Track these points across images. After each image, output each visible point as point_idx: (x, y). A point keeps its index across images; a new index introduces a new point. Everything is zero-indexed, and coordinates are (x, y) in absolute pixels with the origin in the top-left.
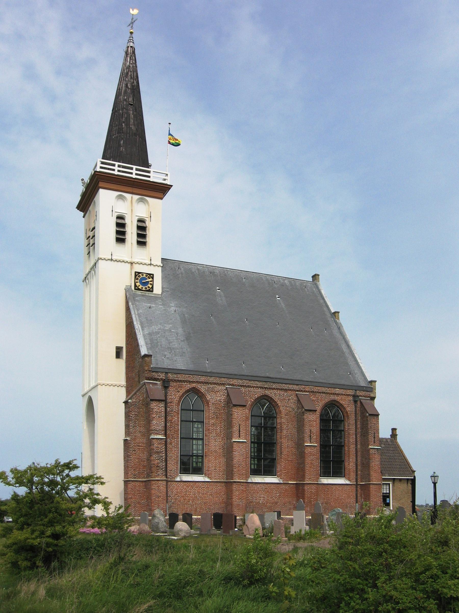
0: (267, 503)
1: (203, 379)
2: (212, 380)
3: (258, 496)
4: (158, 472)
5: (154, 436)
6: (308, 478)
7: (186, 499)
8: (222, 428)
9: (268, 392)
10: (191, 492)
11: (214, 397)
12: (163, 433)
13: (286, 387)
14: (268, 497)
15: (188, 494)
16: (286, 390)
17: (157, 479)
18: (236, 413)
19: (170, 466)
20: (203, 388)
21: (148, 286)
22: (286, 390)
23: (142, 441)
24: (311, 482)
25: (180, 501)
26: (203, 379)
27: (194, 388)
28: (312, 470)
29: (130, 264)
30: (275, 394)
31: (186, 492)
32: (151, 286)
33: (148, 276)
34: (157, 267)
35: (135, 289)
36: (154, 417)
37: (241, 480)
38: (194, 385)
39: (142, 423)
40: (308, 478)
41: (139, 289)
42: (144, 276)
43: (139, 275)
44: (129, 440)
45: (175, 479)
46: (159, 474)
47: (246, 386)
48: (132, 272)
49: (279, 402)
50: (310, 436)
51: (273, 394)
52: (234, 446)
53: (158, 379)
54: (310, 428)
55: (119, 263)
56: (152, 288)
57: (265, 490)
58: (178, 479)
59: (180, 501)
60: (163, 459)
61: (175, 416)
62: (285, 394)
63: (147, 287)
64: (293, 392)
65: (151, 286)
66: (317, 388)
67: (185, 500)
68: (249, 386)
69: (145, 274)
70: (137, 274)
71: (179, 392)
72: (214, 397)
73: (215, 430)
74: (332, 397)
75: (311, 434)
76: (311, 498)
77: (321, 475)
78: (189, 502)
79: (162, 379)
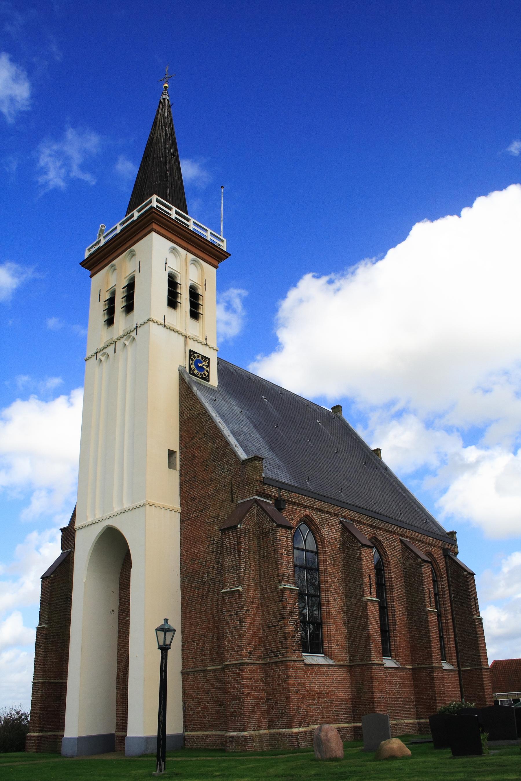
8: (340, 580)
12: (293, 581)
20: (317, 518)
21: (203, 372)
23: (256, 594)
26: (317, 504)
29: (182, 339)
32: (207, 374)
33: (204, 359)
34: (212, 349)
35: (190, 373)
37: (378, 661)
39: (254, 564)
41: (193, 374)
42: (200, 358)
43: (194, 356)
44: (242, 592)
46: (295, 650)
48: (186, 349)
52: (369, 607)
53: (270, 496)
55: (172, 332)
56: (208, 376)
60: (298, 624)
63: (202, 373)
64: (396, 537)
65: (208, 374)
69: (201, 356)
70: (192, 353)
73: (333, 582)
79: (275, 497)
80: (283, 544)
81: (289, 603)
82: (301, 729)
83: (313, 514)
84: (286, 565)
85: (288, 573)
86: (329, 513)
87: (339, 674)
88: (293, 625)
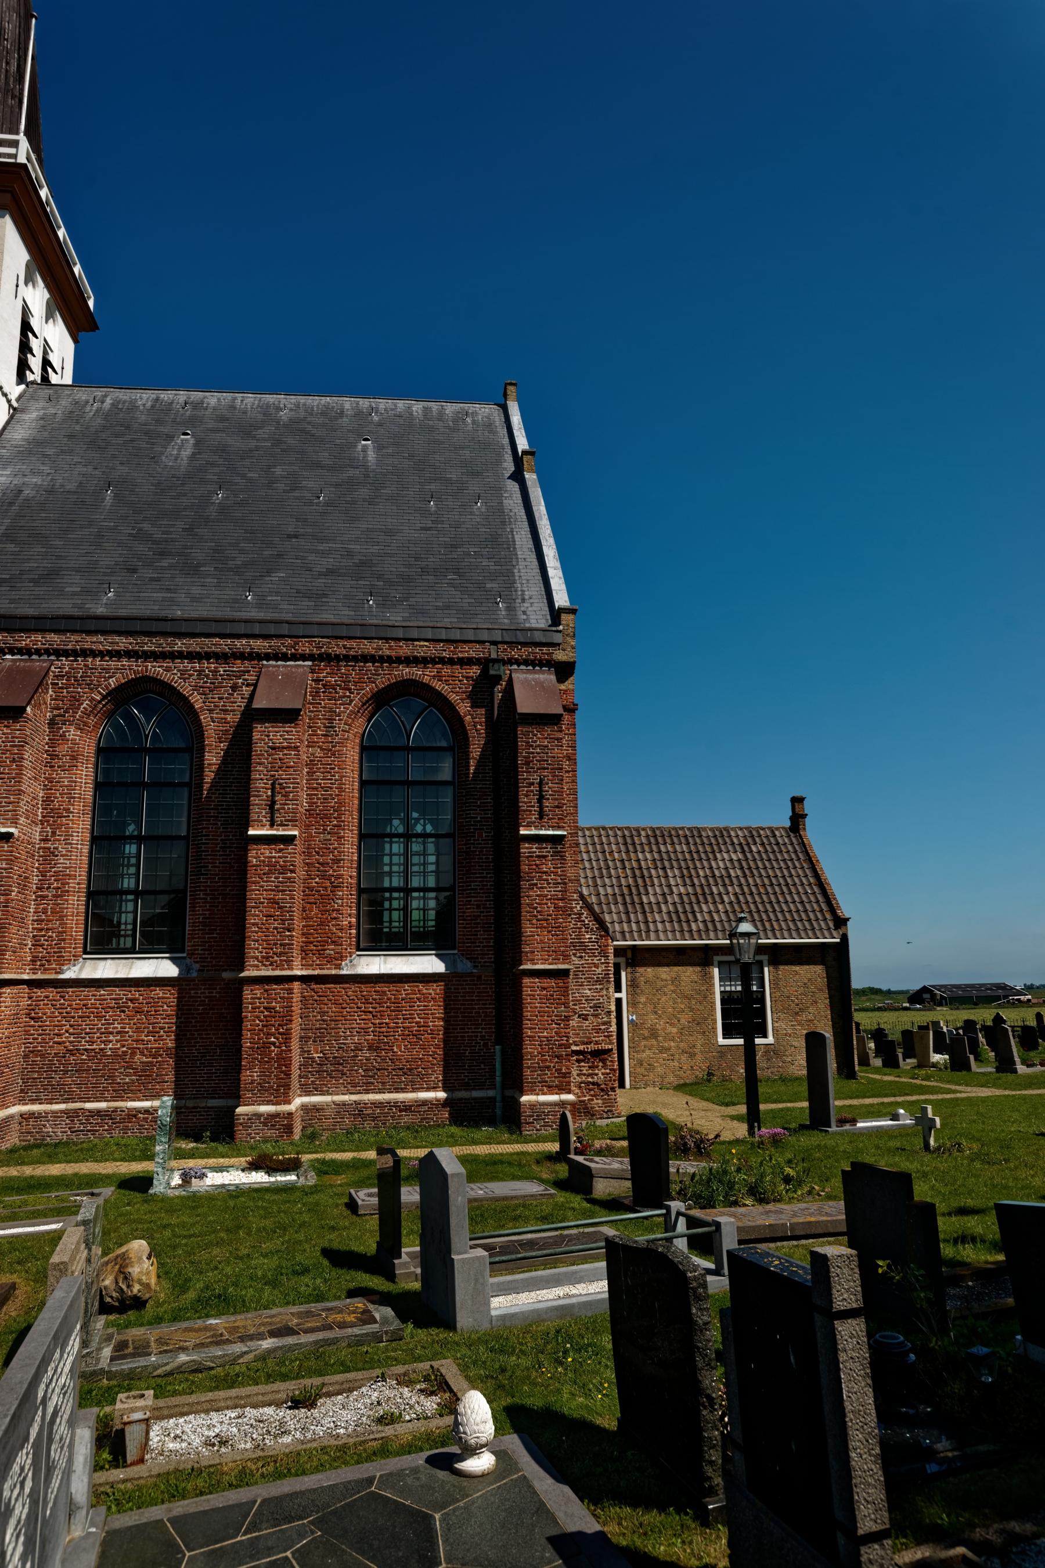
0: (133, 1054)
3: (98, 1029)
6: (257, 958)
9: (155, 669)
13: (223, 645)
14: (138, 1030)
16: (222, 657)
22: (222, 657)
24: (270, 973)
28: (276, 928)
30: (183, 672)
40: (257, 958)
47: (75, 654)
49: (197, 701)
50: (273, 803)
51: (175, 672)
54: (273, 776)
57: (128, 1007)
62: (221, 669)
66: (341, 643)
68: (85, 653)
74: (406, 672)
75: (273, 795)
76: (269, 1034)
77: (362, 945)
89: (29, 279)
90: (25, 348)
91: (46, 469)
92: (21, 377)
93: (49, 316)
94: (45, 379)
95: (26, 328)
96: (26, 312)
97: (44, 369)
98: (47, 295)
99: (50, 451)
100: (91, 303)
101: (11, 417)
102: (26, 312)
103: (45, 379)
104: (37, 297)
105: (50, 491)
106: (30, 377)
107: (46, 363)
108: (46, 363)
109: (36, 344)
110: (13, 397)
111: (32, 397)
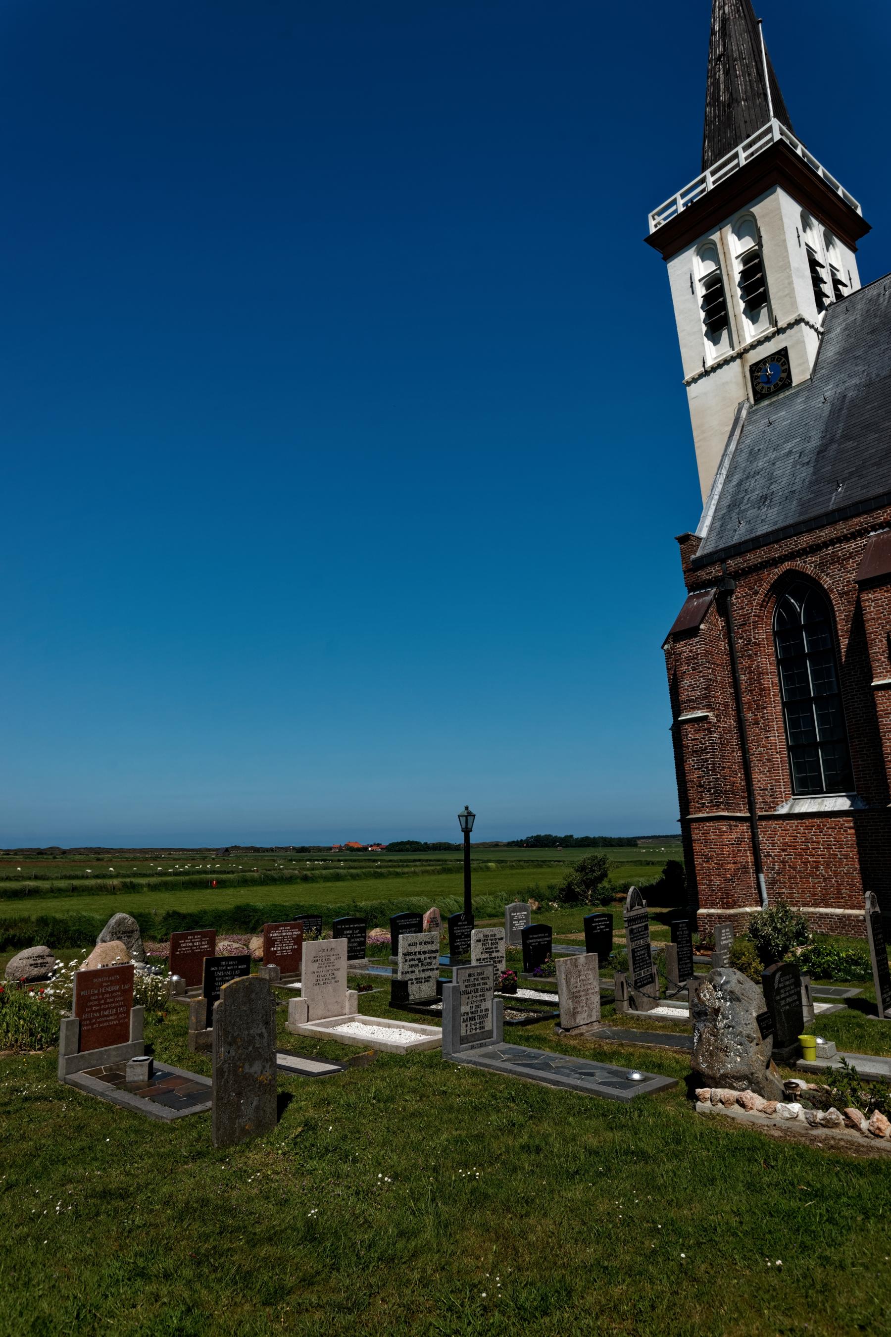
1: (804, 541)
2: (825, 534)
4: (701, 799)
5: (687, 715)
7: (809, 862)
10: (818, 843)
11: (841, 577)
15: (813, 849)
17: (701, 815)
18: (873, 604)
19: (759, 778)
20: (808, 566)
25: (794, 868)
26: (804, 541)
27: (789, 572)
31: (806, 841)
36: (685, 672)
38: (787, 565)
45: (775, 811)
46: (704, 803)
52: (879, 700)
58: (783, 810)
59: (794, 868)
61: (756, 654)
65: (786, 374)
67: (805, 863)
71: (756, 593)
72: (841, 577)
78: (817, 868)
80: (685, 658)
81: (692, 740)
82: (712, 911)
83: (798, 564)
84: (692, 685)
85: (695, 696)
86: (832, 542)
87: (882, 824)
88: (699, 769)
89: (806, 225)
90: (817, 281)
91: (860, 368)
92: (820, 306)
93: (828, 243)
94: (839, 296)
95: (814, 264)
96: (810, 252)
97: (836, 289)
98: (822, 228)
99: (859, 353)
100: (859, 212)
101: (822, 342)
102: (810, 252)
103: (839, 296)
104: (815, 236)
105: (869, 384)
106: (827, 301)
107: (837, 282)
108: (837, 282)
109: (825, 274)
110: (818, 326)
111: (833, 317)
